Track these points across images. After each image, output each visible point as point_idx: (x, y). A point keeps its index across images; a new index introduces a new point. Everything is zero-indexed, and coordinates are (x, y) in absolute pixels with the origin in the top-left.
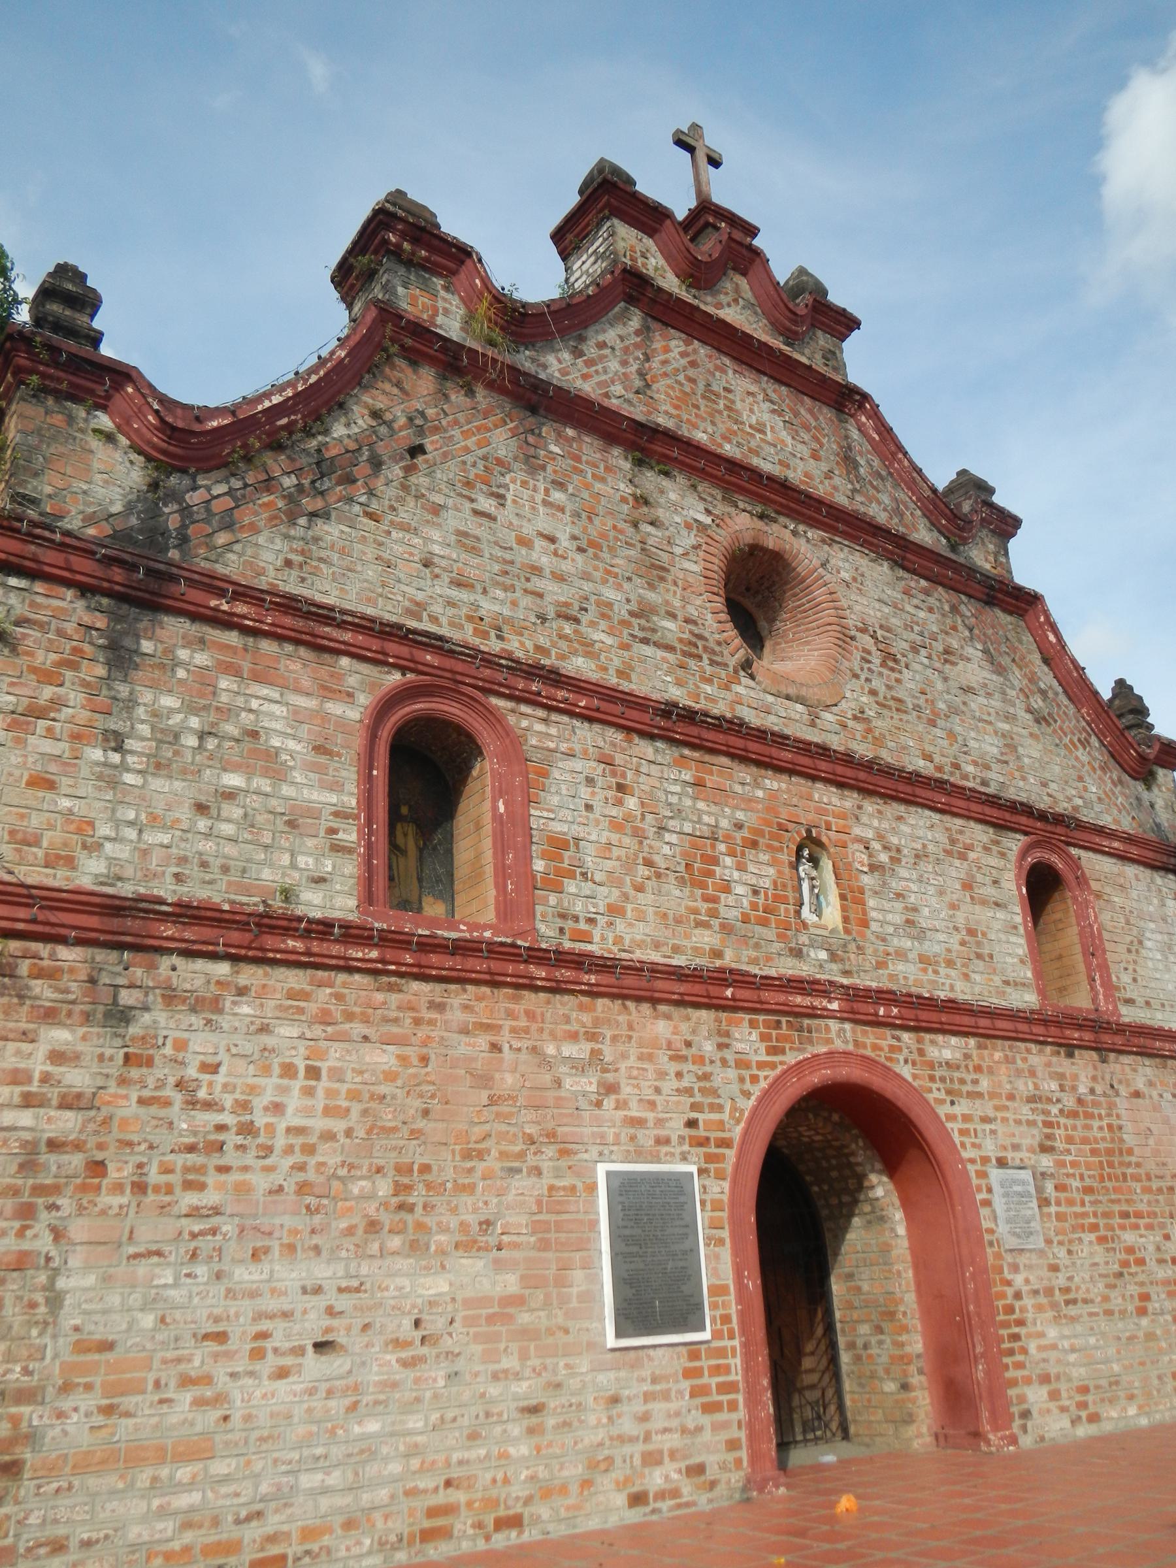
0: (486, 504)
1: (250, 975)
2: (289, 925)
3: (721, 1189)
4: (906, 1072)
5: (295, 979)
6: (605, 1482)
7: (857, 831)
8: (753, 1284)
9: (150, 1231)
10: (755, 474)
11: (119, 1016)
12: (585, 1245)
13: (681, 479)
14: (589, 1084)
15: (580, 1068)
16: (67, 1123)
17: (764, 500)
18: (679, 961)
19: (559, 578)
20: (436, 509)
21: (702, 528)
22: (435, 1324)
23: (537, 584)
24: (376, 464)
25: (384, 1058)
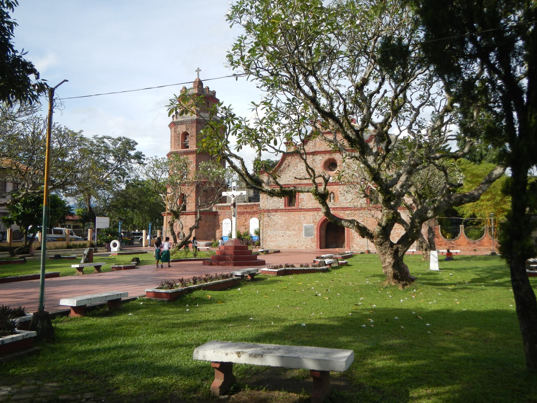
0: (296, 168)
1: (277, 213)
2: (278, 210)
3: (316, 226)
4: (341, 215)
5: (280, 213)
6: (303, 246)
7: (339, 190)
8: (318, 234)
9: (272, 229)
10: (327, 151)
11: (269, 217)
12: (302, 230)
13: (319, 155)
14: (303, 218)
15: (303, 217)
16: (267, 223)
17: (330, 153)
18: (314, 207)
19: (303, 173)
20: (291, 171)
21: (321, 160)
22: (290, 235)
23: (301, 174)
24: (285, 169)
25: (286, 218)
